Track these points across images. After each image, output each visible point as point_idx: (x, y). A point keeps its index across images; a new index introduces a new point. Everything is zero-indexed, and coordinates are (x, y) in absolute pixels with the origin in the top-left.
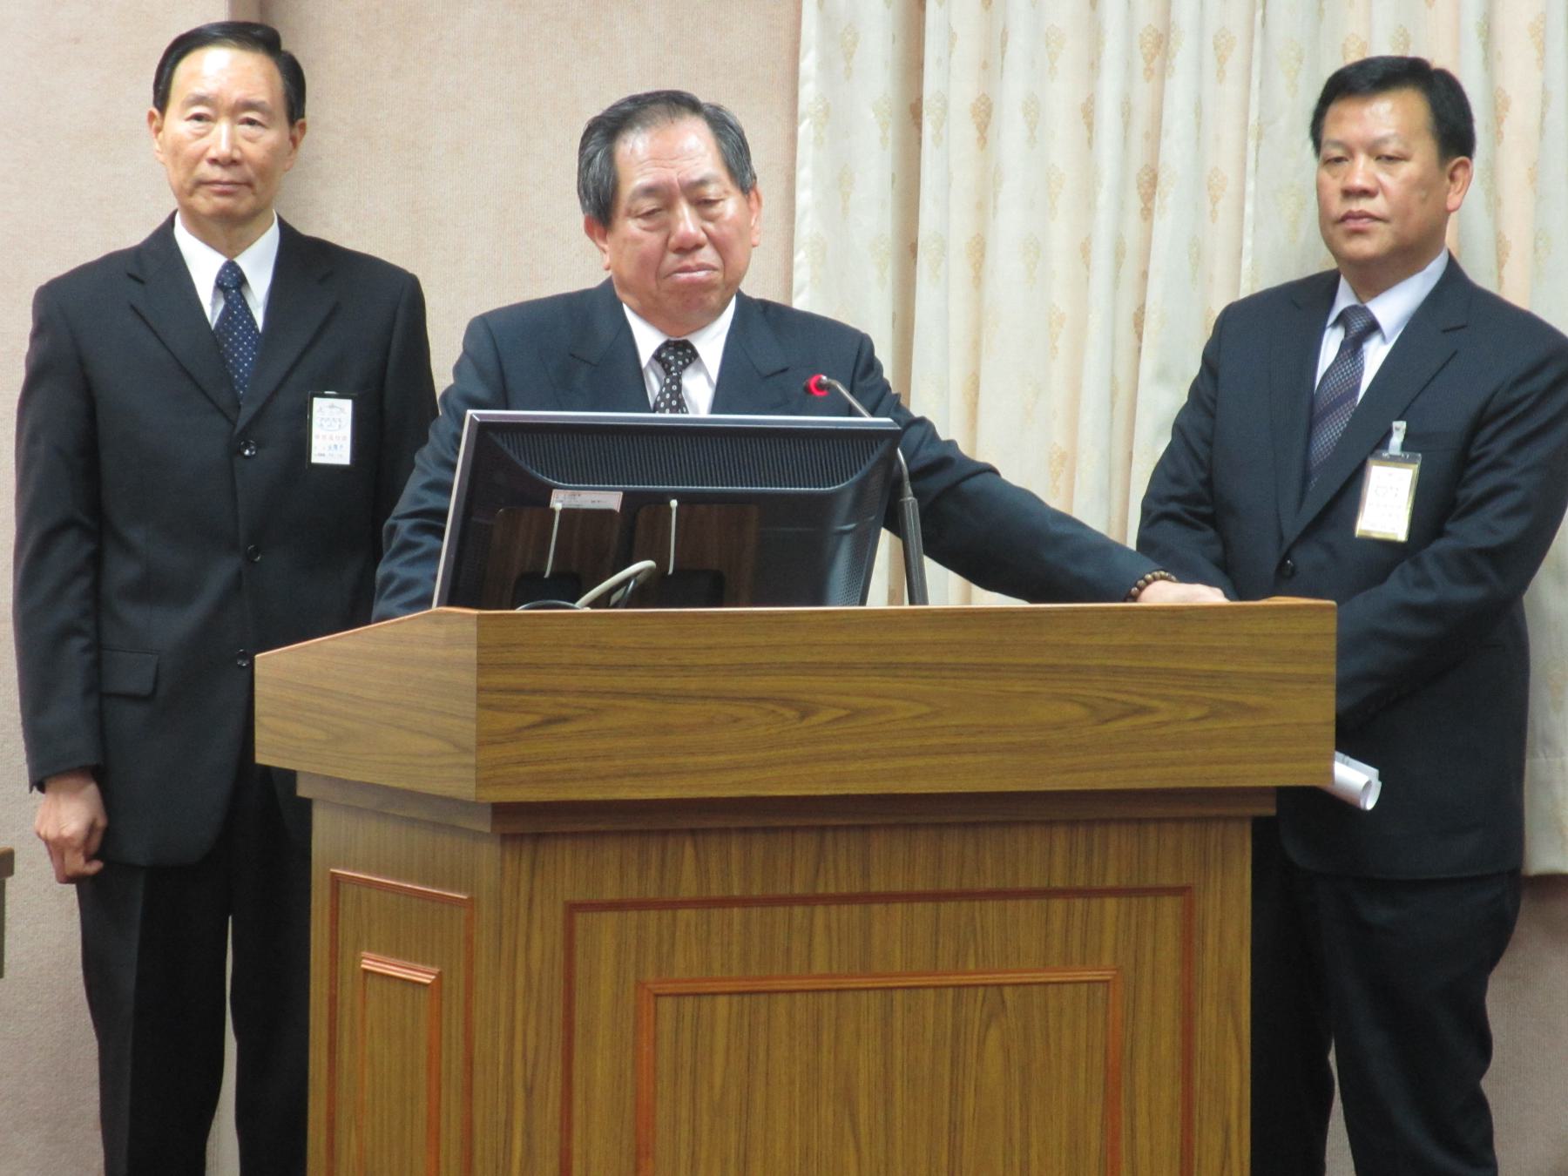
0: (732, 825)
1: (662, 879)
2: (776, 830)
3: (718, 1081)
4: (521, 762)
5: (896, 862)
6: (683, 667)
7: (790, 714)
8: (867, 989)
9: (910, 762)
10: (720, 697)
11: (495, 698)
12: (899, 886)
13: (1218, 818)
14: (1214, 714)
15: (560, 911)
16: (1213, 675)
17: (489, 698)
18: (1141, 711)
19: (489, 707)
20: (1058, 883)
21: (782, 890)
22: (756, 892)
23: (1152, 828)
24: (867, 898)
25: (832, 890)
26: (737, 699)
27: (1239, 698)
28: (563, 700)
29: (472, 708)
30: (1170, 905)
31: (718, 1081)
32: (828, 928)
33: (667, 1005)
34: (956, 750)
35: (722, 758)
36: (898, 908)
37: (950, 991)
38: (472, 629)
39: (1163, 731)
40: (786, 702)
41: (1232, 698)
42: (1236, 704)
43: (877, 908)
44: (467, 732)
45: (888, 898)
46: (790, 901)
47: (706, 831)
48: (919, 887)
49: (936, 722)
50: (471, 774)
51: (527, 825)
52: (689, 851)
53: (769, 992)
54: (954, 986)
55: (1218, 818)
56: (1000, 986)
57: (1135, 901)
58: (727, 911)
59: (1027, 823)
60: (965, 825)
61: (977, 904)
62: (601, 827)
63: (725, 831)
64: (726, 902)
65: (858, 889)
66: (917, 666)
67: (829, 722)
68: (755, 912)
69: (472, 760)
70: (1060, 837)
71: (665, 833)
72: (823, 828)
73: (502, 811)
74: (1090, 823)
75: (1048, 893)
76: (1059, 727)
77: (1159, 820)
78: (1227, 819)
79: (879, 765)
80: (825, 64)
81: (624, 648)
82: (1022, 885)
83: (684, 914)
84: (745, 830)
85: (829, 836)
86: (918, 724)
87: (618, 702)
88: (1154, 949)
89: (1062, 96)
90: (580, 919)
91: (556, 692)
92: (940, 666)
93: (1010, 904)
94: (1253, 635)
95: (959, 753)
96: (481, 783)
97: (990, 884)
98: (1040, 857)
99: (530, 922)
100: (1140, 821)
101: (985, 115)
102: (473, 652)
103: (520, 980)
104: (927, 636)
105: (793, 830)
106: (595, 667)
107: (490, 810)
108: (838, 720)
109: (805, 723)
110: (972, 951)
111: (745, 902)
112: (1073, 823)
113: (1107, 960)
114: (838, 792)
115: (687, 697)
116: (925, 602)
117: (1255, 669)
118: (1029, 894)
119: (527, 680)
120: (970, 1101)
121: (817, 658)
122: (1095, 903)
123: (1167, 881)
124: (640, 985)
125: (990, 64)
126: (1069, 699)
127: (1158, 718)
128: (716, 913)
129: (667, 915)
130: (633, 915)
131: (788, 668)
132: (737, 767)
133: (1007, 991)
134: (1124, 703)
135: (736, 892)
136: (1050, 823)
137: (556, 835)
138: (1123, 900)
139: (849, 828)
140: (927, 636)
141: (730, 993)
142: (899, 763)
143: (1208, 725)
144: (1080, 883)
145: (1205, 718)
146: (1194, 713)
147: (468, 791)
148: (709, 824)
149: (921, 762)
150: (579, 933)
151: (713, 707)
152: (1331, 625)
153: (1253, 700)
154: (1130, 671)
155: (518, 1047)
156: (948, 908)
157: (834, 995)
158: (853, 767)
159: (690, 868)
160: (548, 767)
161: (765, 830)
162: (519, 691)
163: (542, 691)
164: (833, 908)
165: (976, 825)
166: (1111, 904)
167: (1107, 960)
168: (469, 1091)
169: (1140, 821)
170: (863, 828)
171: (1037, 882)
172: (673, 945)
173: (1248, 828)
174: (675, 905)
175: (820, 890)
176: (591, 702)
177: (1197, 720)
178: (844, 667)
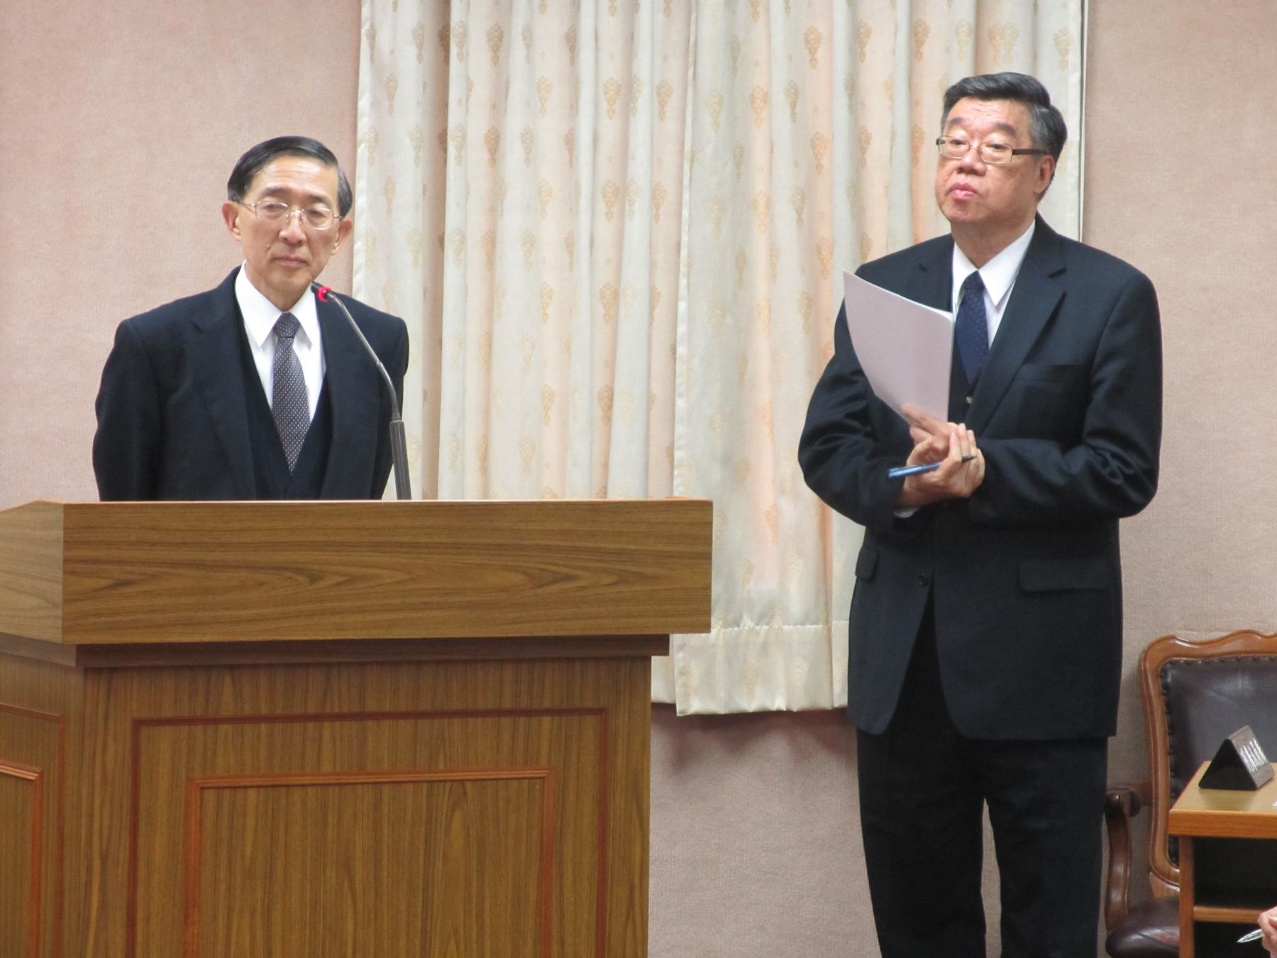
1: (207, 701)
2: (294, 666)
3: (248, 853)
4: (97, 615)
6: (222, 545)
7: (301, 579)
8: (362, 784)
9: (394, 616)
14: (623, 579)
16: (619, 553)
17: (71, 567)
18: (567, 578)
19: (73, 573)
20: (507, 704)
21: (298, 710)
22: (279, 711)
24: (362, 716)
25: (337, 710)
28: (129, 568)
30: (590, 722)
31: (248, 853)
33: (210, 796)
34: (427, 606)
35: (251, 612)
36: (386, 724)
37: (425, 786)
38: (60, 515)
40: (299, 571)
41: (634, 569)
43: (371, 724)
45: (379, 716)
46: (306, 718)
47: (240, 666)
48: (403, 708)
50: (59, 623)
52: (228, 681)
53: (288, 786)
54: (428, 782)
56: (462, 781)
60: (438, 662)
61: (446, 721)
62: (161, 663)
64: (256, 719)
65: (356, 708)
66: (402, 545)
68: (278, 727)
69: (60, 613)
71: (209, 668)
72: (330, 665)
73: (84, 651)
75: (499, 713)
77: (584, 659)
79: (370, 617)
80: (375, 104)
82: (480, 706)
83: (224, 728)
84: (270, 666)
87: (169, 570)
89: (550, 130)
90: (145, 732)
93: (471, 720)
96: (66, 630)
97: (456, 705)
101: (494, 142)
102: (61, 533)
103: (98, 778)
105: (307, 665)
106: (154, 544)
107: (74, 650)
108: (339, 584)
110: (442, 757)
111: (271, 719)
113: (543, 761)
115: (225, 566)
116: (409, 497)
119: (101, 554)
120: (439, 866)
121: (322, 538)
122: (535, 720)
123: (589, 704)
124: (190, 780)
125: (498, 106)
127: (579, 584)
132: (263, 619)
133: (469, 785)
135: (264, 711)
137: (126, 669)
138: (556, 719)
139: (349, 664)
141: (258, 787)
142: (387, 616)
143: (617, 589)
146: (607, 580)
147: (55, 635)
153: (650, 571)
155: (96, 825)
156: (423, 724)
157: (337, 788)
159: (228, 694)
160: (118, 618)
161: (287, 666)
162: (95, 561)
164: (337, 724)
165: (446, 662)
166: (546, 721)
167: (543, 761)
168: (60, 859)
169: (568, 659)
170: (361, 664)
174: (216, 721)
175: (328, 710)
176: (154, 570)
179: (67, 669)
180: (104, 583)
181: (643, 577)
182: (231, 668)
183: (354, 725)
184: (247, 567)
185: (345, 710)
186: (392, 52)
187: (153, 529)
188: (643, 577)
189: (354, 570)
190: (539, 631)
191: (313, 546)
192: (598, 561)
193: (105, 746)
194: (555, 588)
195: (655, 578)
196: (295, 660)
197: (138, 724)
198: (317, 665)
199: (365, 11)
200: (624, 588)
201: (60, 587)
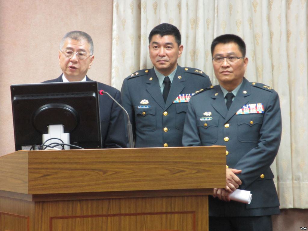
0: (89, 199)
1: (72, 212)
5: (126, 207)
6: (76, 163)
7: (101, 173)
9: (129, 183)
10: (85, 169)
11: (32, 170)
12: (127, 212)
13: (200, 196)
14: (199, 171)
15: (49, 218)
16: (197, 163)
17: (31, 171)
20: (164, 211)
21: (100, 213)
22: (94, 214)
23: (186, 198)
24: (120, 215)
25: (112, 213)
28: (48, 171)
29: (27, 173)
30: (190, 216)
32: (111, 222)
34: (140, 181)
36: (127, 217)
38: (27, 155)
40: (100, 170)
43: (122, 217)
44: (26, 178)
45: (125, 215)
47: (83, 200)
48: (132, 212)
49: (135, 175)
50: (27, 188)
51: (41, 199)
52: (79, 205)
55: (200, 196)
57: (182, 214)
58: (88, 218)
59: (157, 197)
60: (143, 198)
61: (146, 216)
63: (87, 200)
64: (87, 216)
65: (118, 212)
66: (131, 162)
67: (110, 175)
68: (94, 219)
69: (27, 185)
70: (164, 200)
71: (73, 201)
72: (110, 199)
73: (35, 196)
76: (163, 175)
78: (202, 196)
79: (121, 184)
81: (63, 159)
82: (156, 211)
83: (78, 219)
85: (111, 201)
86: (131, 175)
87: (61, 171)
88: (186, 226)
90: (53, 221)
92: (136, 162)
93: (153, 216)
94: (207, 154)
95: (141, 181)
96: (29, 190)
97: (148, 211)
98: (160, 205)
99: (42, 221)
100: (183, 196)
102: (27, 160)
104: (132, 155)
105: (103, 199)
106: (55, 163)
108: (112, 174)
109: (105, 175)
110: (144, 226)
111: (92, 216)
112: (167, 197)
114: (112, 191)
115: (76, 169)
117: (208, 162)
119: (40, 166)
122: (173, 215)
123: (189, 210)
126: (166, 169)
127: (185, 173)
128: (85, 219)
129: (74, 220)
130: (66, 220)
131: (100, 162)
132: (89, 185)
135: (90, 214)
136: (162, 197)
137: (47, 202)
139: (115, 199)
140: (132, 155)
145: (196, 173)
146: (194, 171)
148: (83, 199)
150: (53, 224)
151: (83, 172)
153: (207, 169)
154: (179, 162)
156: (139, 217)
158: (116, 185)
159: (79, 208)
160: (46, 186)
161: (97, 200)
162: (39, 169)
163: (43, 169)
165: (145, 198)
166: (176, 215)
169: (183, 196)
171: (159, 211)
172: (75, 227)
173: (207, 198)
174: (76, 217)
175: (109, 213)
179: (29, 202)
180: (40, 175)
182: (80, 200)
183: (117, 218)
184: (85, 170)
185: (115, 213)
187: (55, 158)
189: (117, 170)
190: (174, 187)
191: (104, 163)
192: (192, 166)
193: (41, 226)
194: (179, 174)
197: (51, 218)
198: (106, 199)
200: (199, 175)
201: (27, 177)
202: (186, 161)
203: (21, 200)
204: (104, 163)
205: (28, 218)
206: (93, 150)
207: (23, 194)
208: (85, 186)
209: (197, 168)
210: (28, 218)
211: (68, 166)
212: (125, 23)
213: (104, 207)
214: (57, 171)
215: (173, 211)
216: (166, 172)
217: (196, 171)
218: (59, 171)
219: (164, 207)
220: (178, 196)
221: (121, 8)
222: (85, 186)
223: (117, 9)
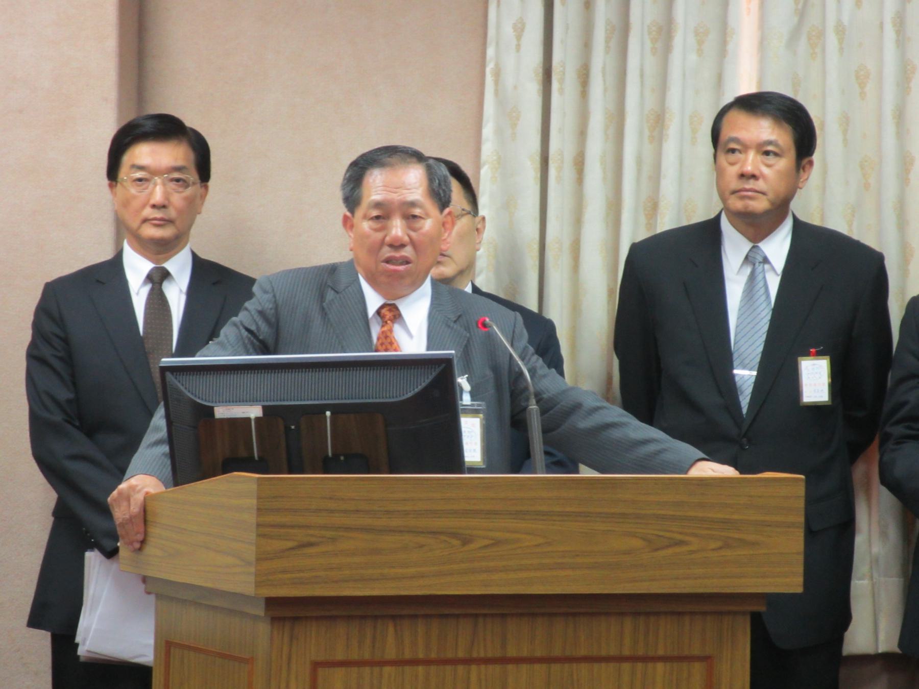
1: (374, 646)
4: (284, 572)
6: (388, 512)
9: (532, 574)
12: (525, 653)
13: (729, 613)
14: (727, 545)
16: (725, 522)
17: (264, 531)
20: (627, 652)
21: (450, 655)
22: (433, 655)
24: (504, 661)
25: (482, 655)
26: (422, 532)
27: (742, 536)
28: (311, 532)
29: (253, 536)
30: (698, 668)
35: (412, 571)
36: (524, 667)
38: (254, 487)
39: (693, 556)
40: (454, 535)
41: (737, 536)
42: (740, 540)
43: (510, 667)
44: (250, 552)
47: (402, 617)
48: (538, 653)
50: (252, 579)
51: (287, 611)
52: (391, 629)
55: (729, 613)
59: (607, 614)
60: (567, 615)
62: (335, 613)
63: (414, 617)
64: (414, 662)
65: (498, 654)
67: (480, 548)
68: (433, 669)
69: (253, 570)
70: (628, 623)
71: (376, 617)
72: (476, 616)
73: (272, 603)
74: (648, 614)
77: (692, 613)
78: (735, 613)
82: (604, 653)
83: (387, 669)
84: (426, 616)
85: (481, 620)
90: (321, 672)
91: (308, 527)
93: (596, 666)
96: (258, 584)
97: (583, 652)
100: (680, 614)
102: (255, 502)
105: (457, 616)
106: (332, 511)
108: (486, 547)
109: (466, 548)
111: (427, 662)
112: (636, 614)
118: (608, 659)
122: (650, 665)
123: (696, 652)
128: (407, 669)
129: (376, 669)
130: (355, 670)
132: (422, 576)
134: (669, 538)
135: (421, 656)
136: (623, 614)
137: (307, 618)
138: (668, 665)
139: (492, 615)
142: (524, 575)
144: (641, 652)
145: (720, 548)
147: (250, 590)
148: (404, 612)
149: (538, 574)
150: (320, 681)
152: (801, 490)
153: (751, 537)
156: (556, 668)
158: (496, 577)
159: (391, 640)
164: (483, 667)
165: (574, 615)
166: (660, 666)
171: (613, 651)
175: (475, 655)
176: (329, 534)
177: (713, 550)
178: (490, 514)
179: (255, 618)
180: (290, 544)
181: (743, 543)
182: (393, 617)
183: (496, 669)
184: (408, 532)
185: (490, 655)
186: (515, 87)
187: (331, 498)
188: (743, 543)
189: (498, 535)
191: (465, 513)
194: (670, 551)
195: (753, 544)
196: (447, 612)
198: (465, 616)
199: (490, 52)
200: (728, 553)
201: (254, 548)
202: (692, 513)
203: (231, 612)
204: (465, 513)
205: (250, 661)
206: (438, 479)
207: (242, 595)
208: (412, 577)
209: (723, 534)
210: (250, 661)
211: (367, 521)
212: (518, 119)
213: (460, 638)
214: (333, 533)
215: (651, 653)
216: (638, 543)
217: (719, 544)
218: (341, 534)
219: (627, 641)
220: (666, 613)
221: (509, 79)
222: (412, 577)
223: (497, 82)
